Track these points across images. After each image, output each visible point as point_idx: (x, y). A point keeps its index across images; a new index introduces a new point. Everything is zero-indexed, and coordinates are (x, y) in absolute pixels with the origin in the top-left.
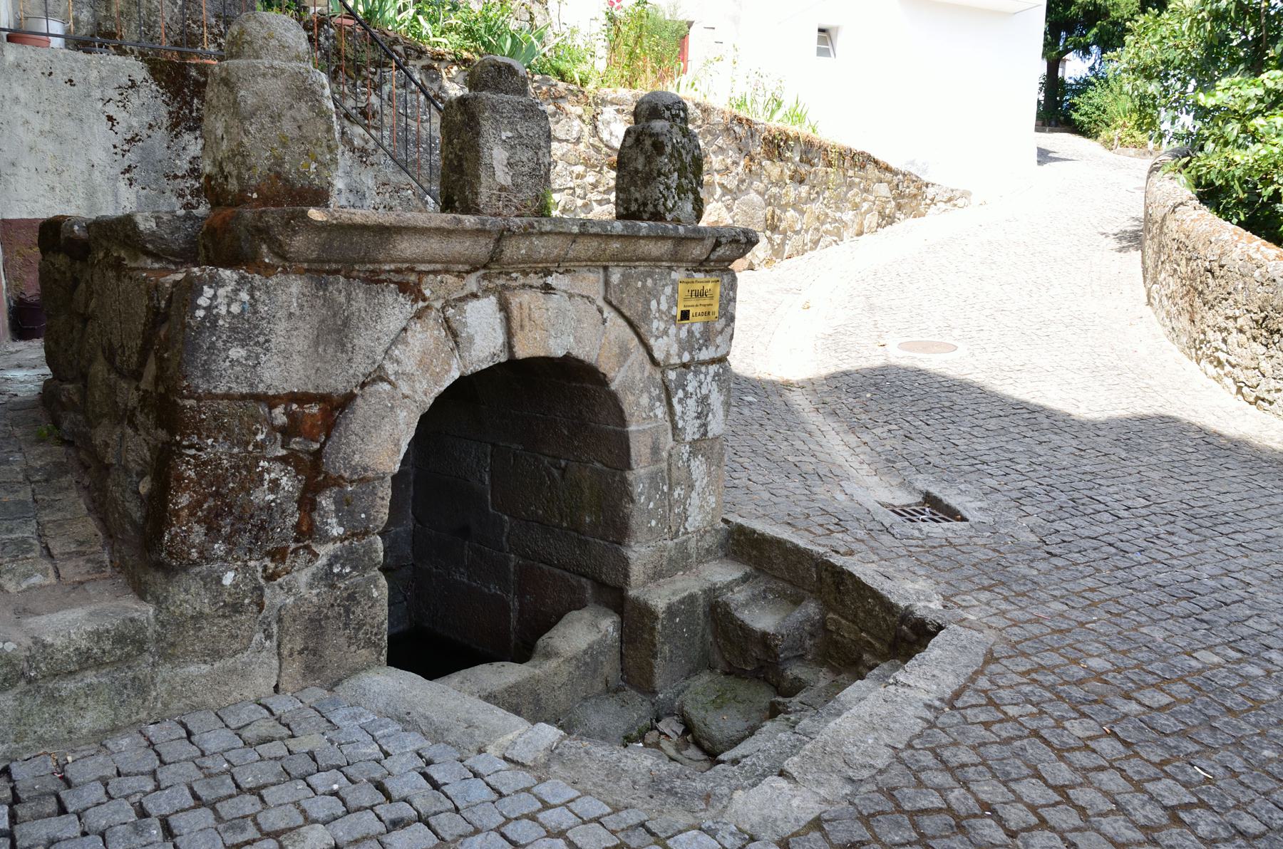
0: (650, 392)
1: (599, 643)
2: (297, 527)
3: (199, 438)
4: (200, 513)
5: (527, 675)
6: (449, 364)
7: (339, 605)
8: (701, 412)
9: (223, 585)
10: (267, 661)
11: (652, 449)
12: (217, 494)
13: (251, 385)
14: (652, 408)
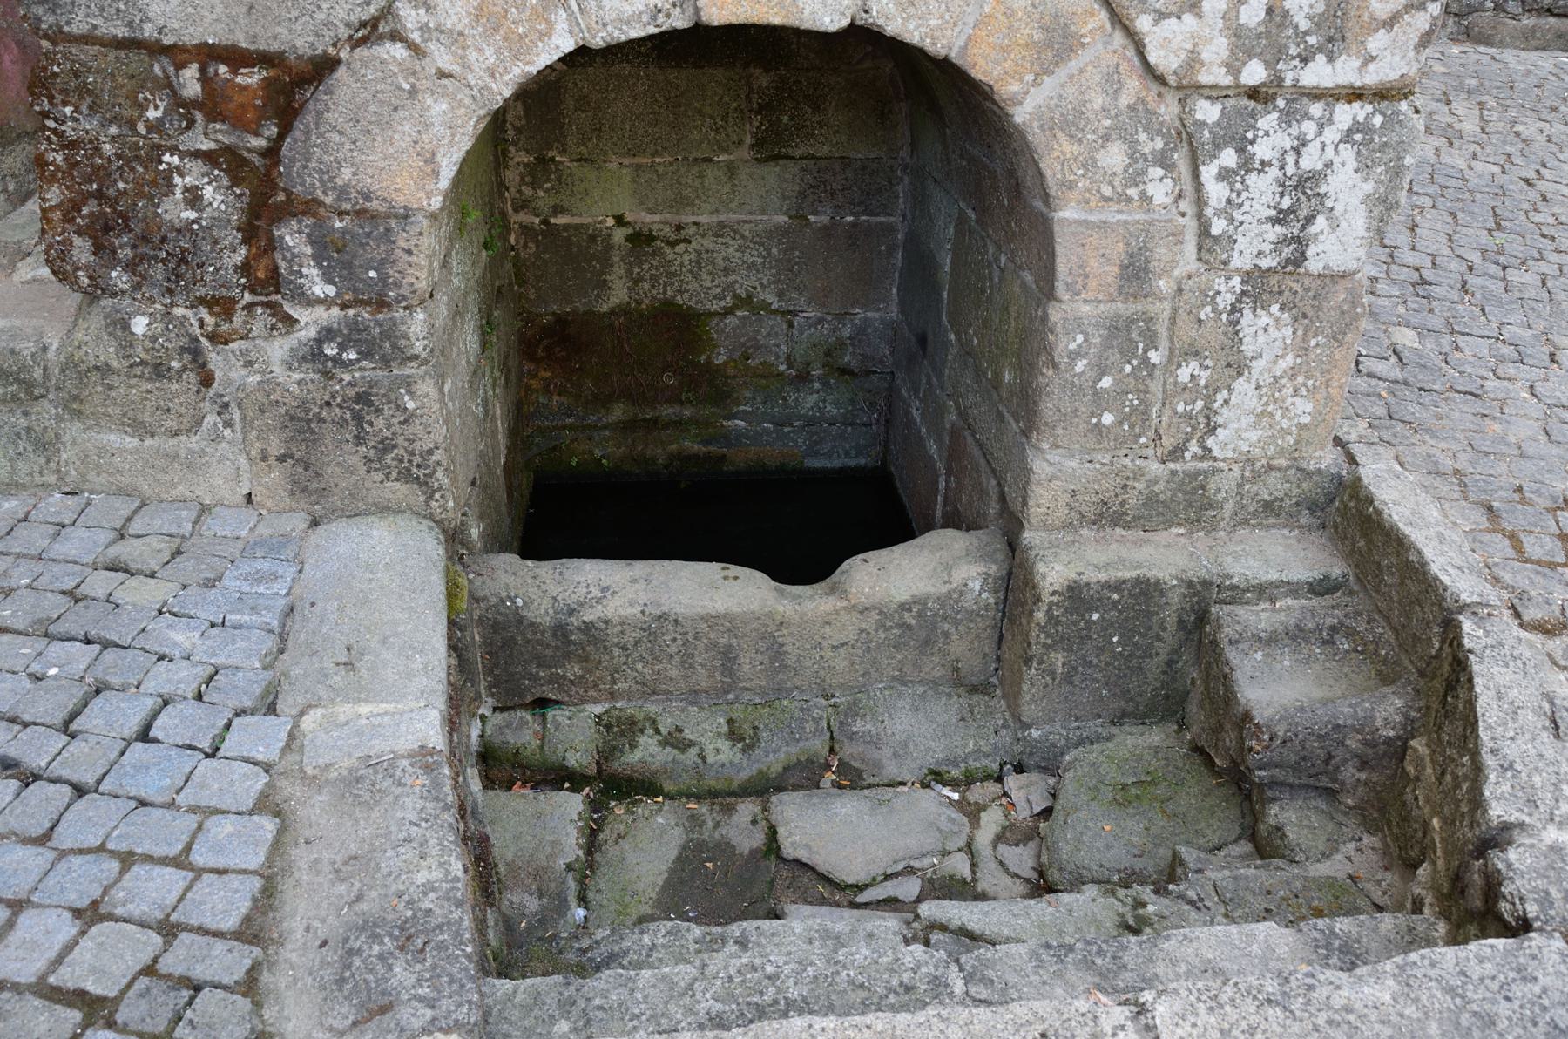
0: (1132, 143)
1: (942, 600)
2: (245, 269)
3: (51, 103)
4: (79, 220)
5: (755, 606)
6: (548, 21)
7: (339, 406)
8: (1291, 210)
9: (133, 334)
10: (231, 456)
11: (1124, 267)
12: (99, 196)
13: (130, 24)
14: (1136, 179)
